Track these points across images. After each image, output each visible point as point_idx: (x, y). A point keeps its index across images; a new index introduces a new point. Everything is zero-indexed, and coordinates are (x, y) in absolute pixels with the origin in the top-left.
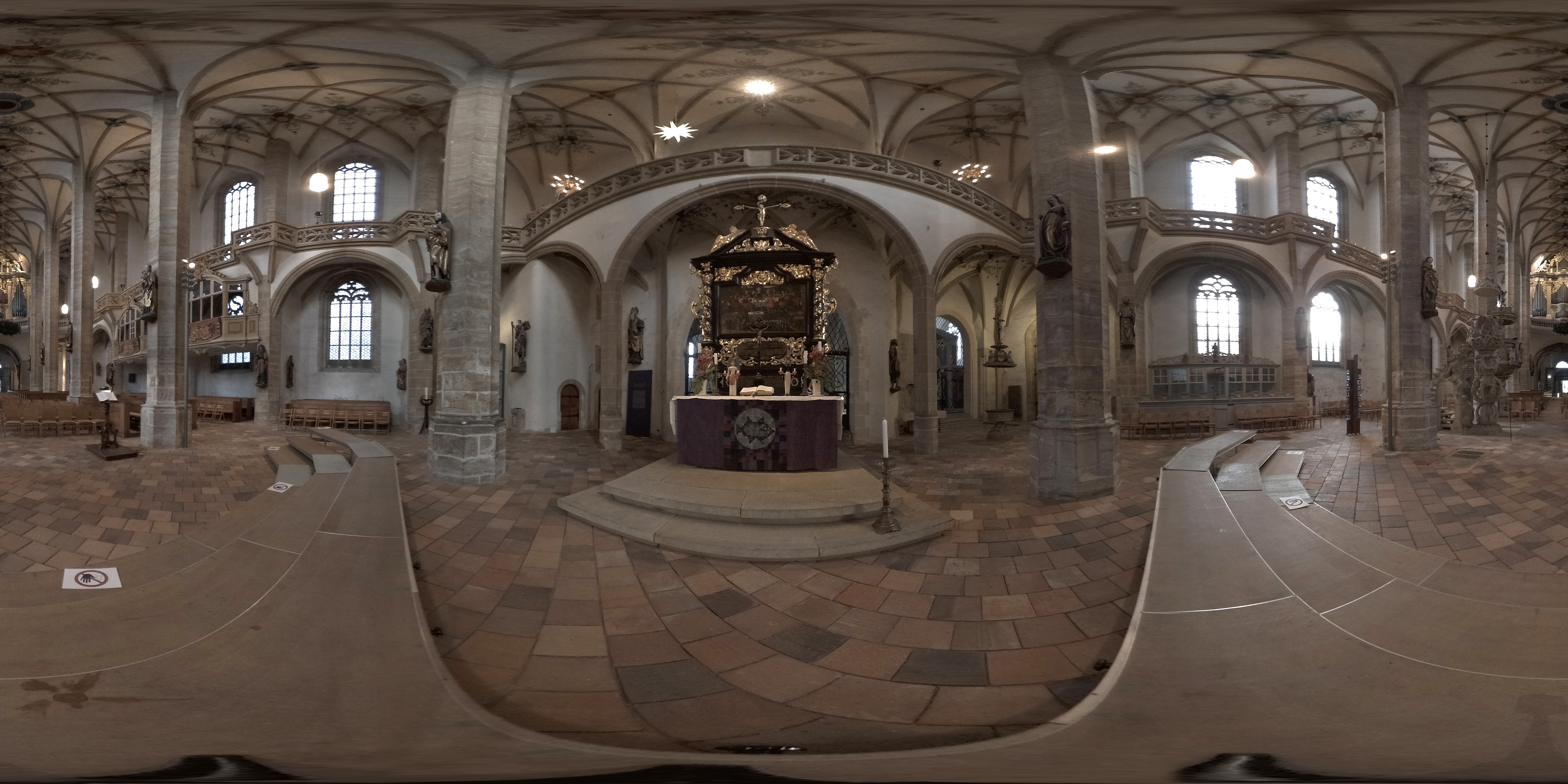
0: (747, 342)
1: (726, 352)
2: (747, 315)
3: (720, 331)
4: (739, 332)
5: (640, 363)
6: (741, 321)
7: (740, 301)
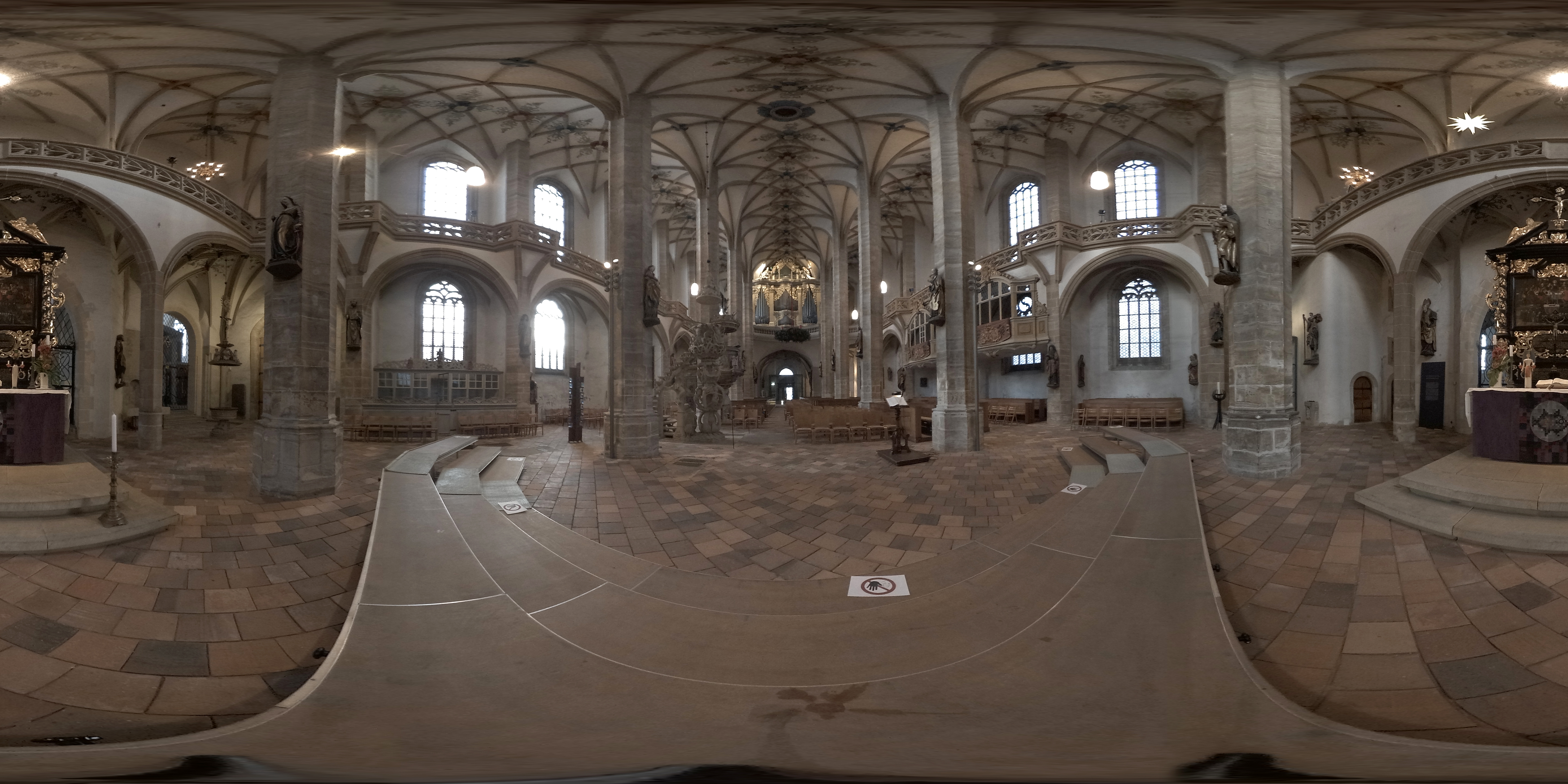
3: (1515, 324)
5: (1433, 355)
7: (1536, 293)
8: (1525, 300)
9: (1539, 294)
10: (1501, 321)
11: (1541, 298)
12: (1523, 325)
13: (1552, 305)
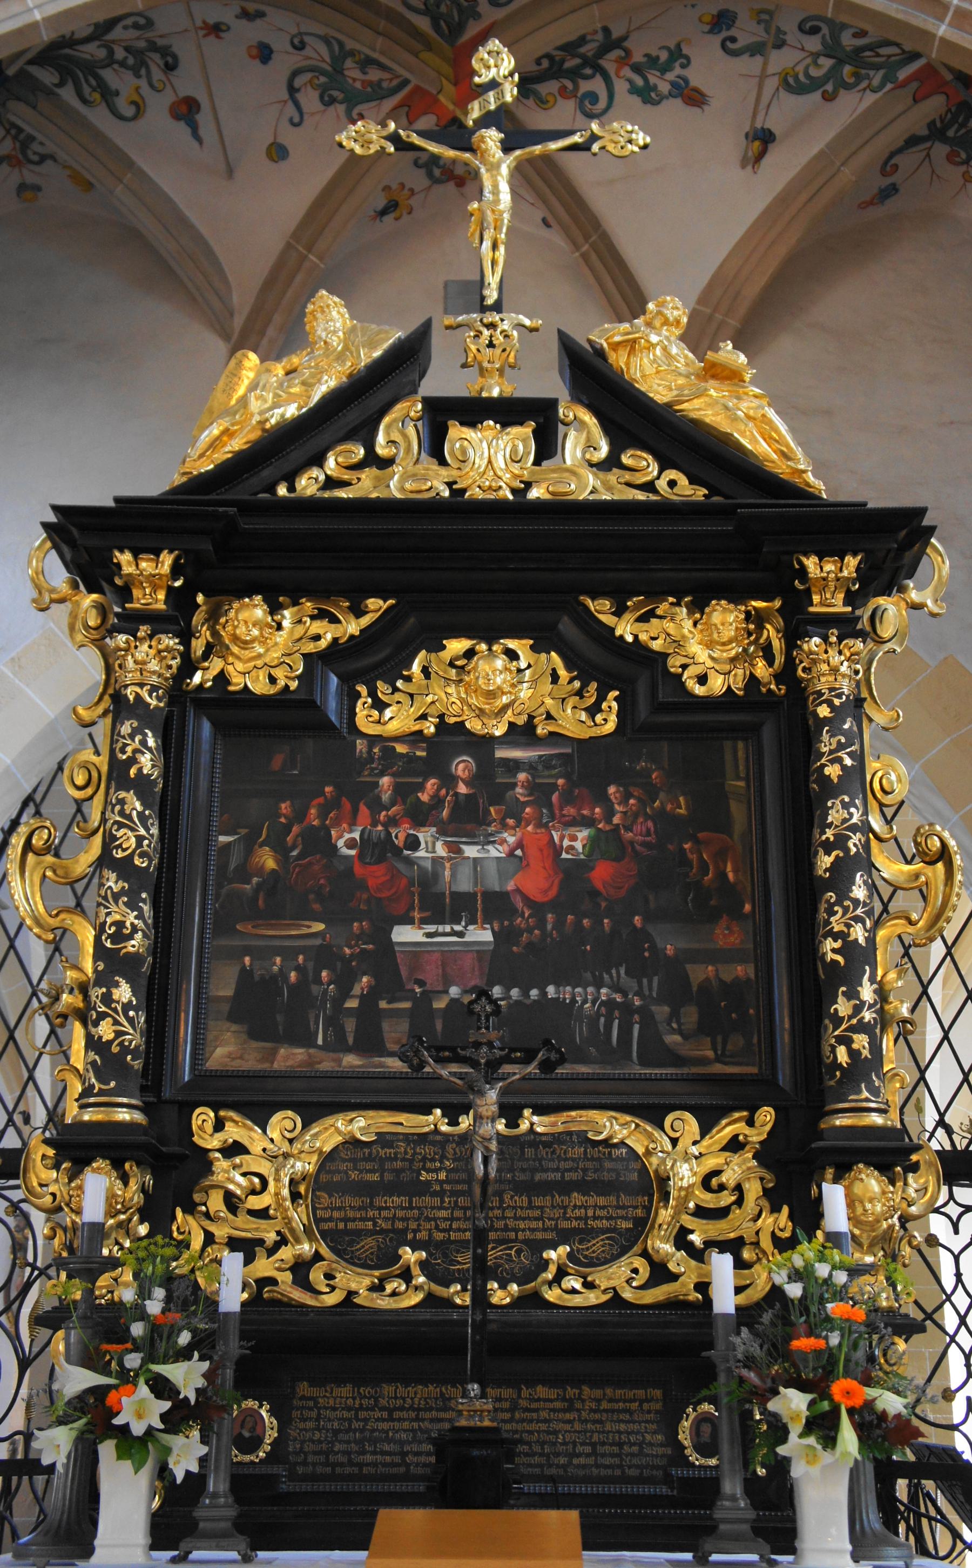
0: (383, 1139)
1: (232, 1203)
2: (390, 945)
4: (327, 1065)
6: (345, 984)
8: (273, 882)
9: (365, 845)
10: (105, 1030)
11: (375, 875)
12: (251, 1062)
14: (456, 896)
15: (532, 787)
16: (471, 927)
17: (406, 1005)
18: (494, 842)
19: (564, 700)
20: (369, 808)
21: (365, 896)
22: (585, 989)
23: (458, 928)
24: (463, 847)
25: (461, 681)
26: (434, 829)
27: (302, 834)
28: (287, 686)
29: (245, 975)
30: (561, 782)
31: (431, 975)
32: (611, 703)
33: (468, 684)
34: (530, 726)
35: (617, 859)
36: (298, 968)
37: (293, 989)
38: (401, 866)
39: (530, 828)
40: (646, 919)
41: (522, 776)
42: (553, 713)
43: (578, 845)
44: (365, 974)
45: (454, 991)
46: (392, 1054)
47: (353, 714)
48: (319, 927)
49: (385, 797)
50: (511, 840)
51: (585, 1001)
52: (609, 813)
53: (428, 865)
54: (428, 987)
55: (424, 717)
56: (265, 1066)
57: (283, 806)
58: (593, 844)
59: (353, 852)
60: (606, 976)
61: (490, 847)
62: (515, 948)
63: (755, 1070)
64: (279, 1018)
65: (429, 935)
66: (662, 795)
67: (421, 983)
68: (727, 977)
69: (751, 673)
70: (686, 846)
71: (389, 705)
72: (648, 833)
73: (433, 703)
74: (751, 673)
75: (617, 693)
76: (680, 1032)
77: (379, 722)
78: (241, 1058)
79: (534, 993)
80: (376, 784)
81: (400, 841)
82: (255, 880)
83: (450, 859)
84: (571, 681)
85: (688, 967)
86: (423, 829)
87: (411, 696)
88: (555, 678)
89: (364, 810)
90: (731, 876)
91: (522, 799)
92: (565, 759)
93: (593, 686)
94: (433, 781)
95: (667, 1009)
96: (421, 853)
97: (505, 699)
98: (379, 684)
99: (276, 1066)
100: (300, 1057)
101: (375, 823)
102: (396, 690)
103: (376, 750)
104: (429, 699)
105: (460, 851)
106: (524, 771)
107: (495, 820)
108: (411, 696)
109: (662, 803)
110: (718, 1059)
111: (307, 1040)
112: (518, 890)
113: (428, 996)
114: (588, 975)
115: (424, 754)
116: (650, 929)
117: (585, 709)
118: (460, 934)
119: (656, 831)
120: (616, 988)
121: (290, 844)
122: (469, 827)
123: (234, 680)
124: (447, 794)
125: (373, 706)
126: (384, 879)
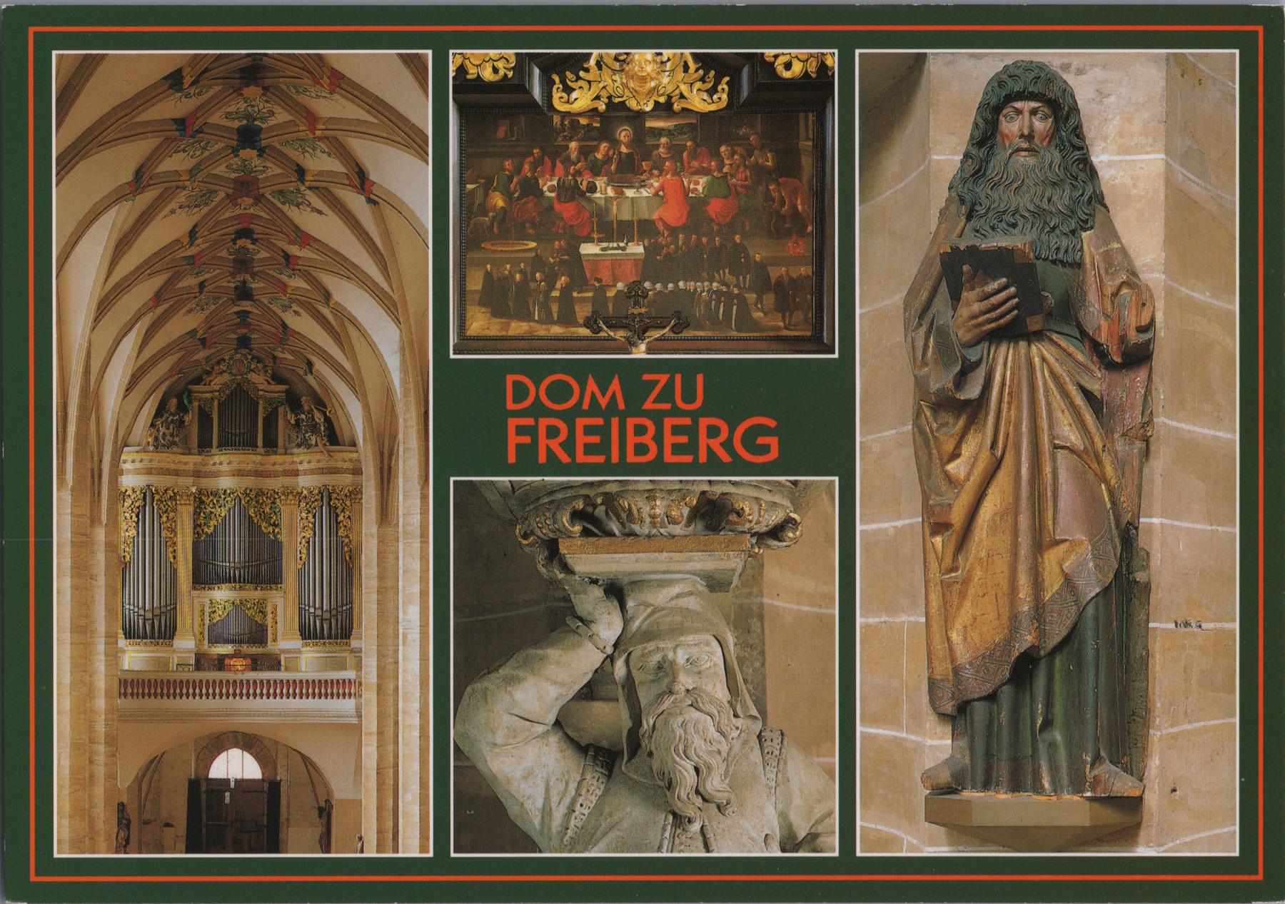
9: (561, 189)
11: (567, 211)
13: (613, 249)
14: (620, 223)
15: (670, 147)
16: (630, 244)
17: (590, 294)
18: (644, 186)
19: (692, 84)
20: (562, 163)
21: (562, 224)
22: (703, 282)
23: (622, 245)
24: (624, 190)
25: (623, 70)
26: (606, 178)
27: (519, 182)
28: (506, 75)
29: (488, 276)
30: (689, 144)
31: (606, 276)
32: (724, 86)
33: (627, 72)
34: (668, 105)
35: (725, 198)
36: (521, 271)
37: (519, 285)
38: (585, 204)
39: (668, 176)
40: (743, 238)
41: (663, 140)
42: (685, 94)
43: (700, 188)
44: (563, 275)
45: (620, 286)
46: (580, 326)
47: (550, 96)
48: (533, 245)
49: (574, 156)
50: (656, 184)
51: (703, 291)
52: (722, 165)
53: (602, 203)
54: (603, 283)
55: (598, 98)
56: (504, 333)
57: (507, 163)
58: (710, 187)
59: (553, 195)
60: (716, 275)
61: (642, 190)
62: (658, 257)
63: (809, 334)
64: (511, 304)
65: (603, 249)
66: (756, 152)
67: (599, 280)
68: (794, 275)
69: (822, 61)
70: (771, 188)
71: (574, 90)
72: (746, 179)
73: (604, 87)
74: (822, 61)
75: (727, 79)
76: (763, 311)
77: (568, 102)
78: (488, 329)
79: (671, 286)
80: (567, 147)
81: (584, 187)
82: (491, 214)
83: (616, 198)
84: (697, 70)
85: (769, 268)
86: (598, 178)
87: (589, 82)
88: (686, 68)
89: (559, 165)
90: (800, 208)
91: (664, 156)
92: (692, 127)
93: (712, 73)
94: (605, 144)
95: (754, 296)
96: (598, 195)
97: (653, 84)
98: (568, 73)
99: (511, 333)
100: (523, 328)
101: (567, 173)
102: (579, 78)
103: (566, 123)
104: (601, 85)
105: (622, 193)
106: (665, 136)
107: (645, 171)
108: (589, 82)
109: (756, 158)
110: (786, 328)
111: (528, 317)
112: (661, 219)
113: (603, 289)
114: (705, 274)
115: (598, 125)
116: (745, 243)
117: (707, 91)
118: (624, 249)
119: (751, 177)
120: (723, 283)
121: (512, 189)
122: (629, 176)
123: (471, 71)
124: (614, 154)
125: (563, 91)
126: (573, 212)
